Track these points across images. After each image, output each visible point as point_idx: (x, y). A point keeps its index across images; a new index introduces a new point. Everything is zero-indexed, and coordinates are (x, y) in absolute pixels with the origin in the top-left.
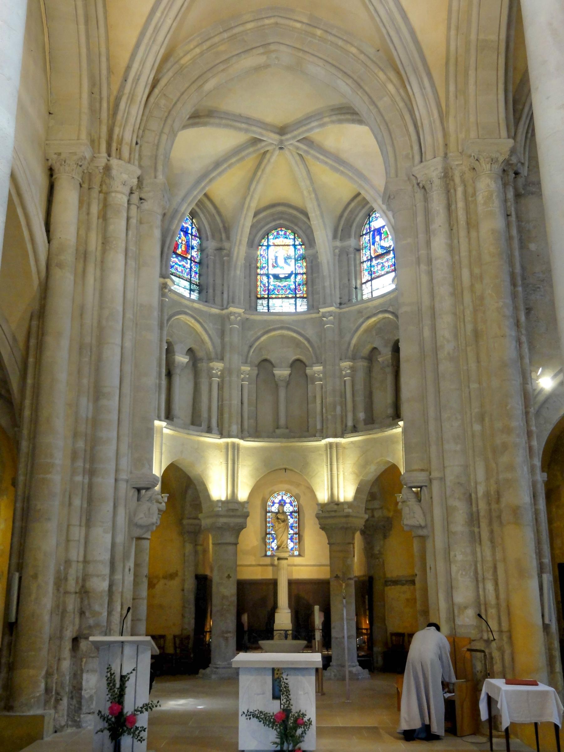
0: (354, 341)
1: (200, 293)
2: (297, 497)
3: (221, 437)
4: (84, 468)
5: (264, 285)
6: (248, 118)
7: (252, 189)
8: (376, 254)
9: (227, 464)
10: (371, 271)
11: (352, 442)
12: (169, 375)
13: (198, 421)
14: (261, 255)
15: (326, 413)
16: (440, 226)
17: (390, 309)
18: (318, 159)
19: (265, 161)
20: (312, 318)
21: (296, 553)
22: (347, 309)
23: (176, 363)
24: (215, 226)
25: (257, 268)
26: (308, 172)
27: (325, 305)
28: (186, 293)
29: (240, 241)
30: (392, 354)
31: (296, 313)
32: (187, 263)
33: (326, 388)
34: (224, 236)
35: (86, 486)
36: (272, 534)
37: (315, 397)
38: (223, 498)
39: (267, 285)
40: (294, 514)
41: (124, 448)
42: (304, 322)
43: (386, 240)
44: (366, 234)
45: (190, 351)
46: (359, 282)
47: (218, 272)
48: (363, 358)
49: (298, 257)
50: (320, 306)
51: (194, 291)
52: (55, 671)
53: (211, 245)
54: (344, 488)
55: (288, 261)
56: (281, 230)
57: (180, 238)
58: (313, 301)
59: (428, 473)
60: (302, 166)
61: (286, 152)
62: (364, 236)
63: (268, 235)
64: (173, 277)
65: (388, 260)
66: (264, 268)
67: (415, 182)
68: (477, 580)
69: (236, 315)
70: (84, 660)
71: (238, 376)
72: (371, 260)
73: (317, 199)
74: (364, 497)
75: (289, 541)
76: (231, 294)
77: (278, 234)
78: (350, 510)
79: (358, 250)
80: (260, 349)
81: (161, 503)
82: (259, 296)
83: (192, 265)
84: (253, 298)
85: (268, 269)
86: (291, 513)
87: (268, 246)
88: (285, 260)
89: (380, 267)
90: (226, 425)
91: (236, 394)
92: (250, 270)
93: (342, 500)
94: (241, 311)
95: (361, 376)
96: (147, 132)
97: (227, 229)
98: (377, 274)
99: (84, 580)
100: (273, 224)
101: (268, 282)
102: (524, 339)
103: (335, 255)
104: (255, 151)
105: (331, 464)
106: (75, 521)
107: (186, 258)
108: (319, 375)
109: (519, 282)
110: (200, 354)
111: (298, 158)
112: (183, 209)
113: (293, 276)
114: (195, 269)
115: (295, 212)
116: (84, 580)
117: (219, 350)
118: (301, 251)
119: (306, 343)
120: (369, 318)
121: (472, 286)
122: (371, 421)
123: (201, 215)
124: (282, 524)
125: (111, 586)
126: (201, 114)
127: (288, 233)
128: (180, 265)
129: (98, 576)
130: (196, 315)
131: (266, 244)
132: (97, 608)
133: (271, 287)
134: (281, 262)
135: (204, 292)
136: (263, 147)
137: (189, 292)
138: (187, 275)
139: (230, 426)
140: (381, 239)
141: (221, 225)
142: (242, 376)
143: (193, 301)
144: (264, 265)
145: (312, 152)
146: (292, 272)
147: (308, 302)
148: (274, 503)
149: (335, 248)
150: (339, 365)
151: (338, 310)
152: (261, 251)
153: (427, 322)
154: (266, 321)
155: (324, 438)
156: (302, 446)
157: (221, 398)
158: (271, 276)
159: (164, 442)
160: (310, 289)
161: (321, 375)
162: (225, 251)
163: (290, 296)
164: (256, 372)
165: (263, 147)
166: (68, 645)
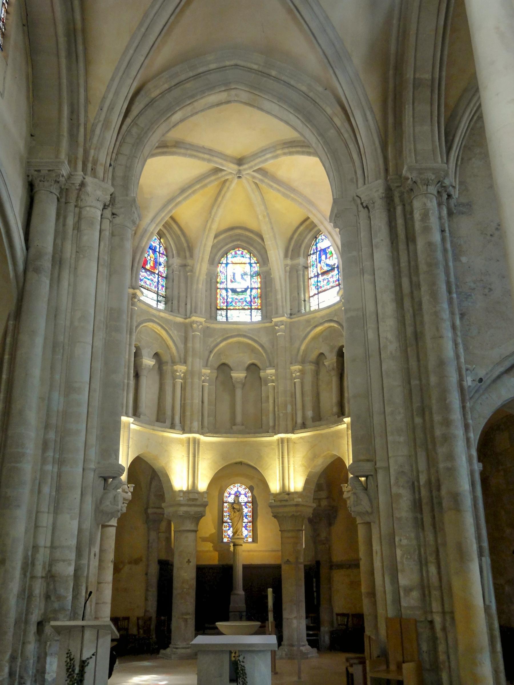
0: (303, 347)
1: (165, 304)
2: (251, 489)
3: (183, 433)
4: (54, 458)
5: (224, 299)
6: (210, 150)
7: (213, 214)
8: (322, 271)
9: (189, 457)
10: (318, 286)
11: (301, 438)
12: (137, 376)
13: (162, 418)
14: (221, 272)
15: (278, 411)
16: (382, 240)
17: (335, 319)
18: (271, 187)
19: (225, 189)
20: (266, 327)
21: (250, 540)
22: (296, 319)
23: (144, 365)
24: (181, 246)
25: (217, 283)
26: (263, 199)
27: (277, 315)
28: (154, 304)
29: (202, 258)
30: (337, 358)
31: (252, 323)
32: (155, 278)
33: (278, 388)
34: (188, 254)
35: (56, 475)
36: (228, 522)
37: (268, 397)
38: (185, 489)
39: (226, 298)
40: (248, 504)
41: (93, 440)
42: (258, 330)
43: (331, 258)
44: (313, 254)
45: (157, 355)
46: (307, 296)
47: (182, 285)
48: (311, 362)
49: (253, 274)
50: (272, 316)
51: (160, 302)
52: (19, 655)
53: (176, 262)
54: (294, 479)
55: (245, 277)
56: (239, 250)
57: (149, 255)
58: (266, 312)
59: (373, 463)
60: (257, 193)
61: (243, 180)
62: (312, 256)
63: (227, 254)
64: (142, 289)
65: (332, 277)
66: (223, 283)
67: (359, 202)
68: (422, 563)
69: (198, 324)
70: (48, 643)
71: (199, 379)
72: (318, 276)
73: (271, 223)
74: (313, 487)
75: (244, 529)
76: (193, 305)
77: (236, 253)
78: (300, 500)
79: (306, 268)
80: (219, 354)
81: (127, 493)
82: (218, 308)
83: (159, 279)
84: (213, 309)
85: (226, 284)
86: (246, 503)
87: (227, 264)
88: (242, 276)
89: (326, 282)
90: (188, 422)
91: (197, 394)
92: (211, 285)
93: (292, 490)
94: (203, 320)
95: (309, 378)
96: (119, 156)
97: (191, 249)
98: (323, 289)
99: (50, 565)
100: (232, 244)
101: (227, 295)
102: (459, 340)
103: (286, 272)
104: (216, 179)
105: (283, 458)
106: (44, 508)
107: (154, 273)
108: (271, 377)
109: (454, 290)
110: (166, 358)
111: (254, 186)
112: (152, 228)
113: (249, 290)
114: (163, 282)
115: (251, 235)
116: (50, 565)
117: (182, 356)
118: (256, 268)
119: (260, 349)
120: (316, 327)
121: (412, 292)
122: (318, 419)
123: (168, 236)
124: (238, 513)
125: (76, 570)
126: (168, 144)
127: (244, 253)
128: (148, 279)
129: (64, 561)
130: (164, 324)
131: (225, 262)
132: (62, 592)
133: (229, 300)
134: (238, 277)
135: (170, 303)
136: (222, 176)
137: (156, 302)
138: (155, 287)
139: (191, 423)
140: (326, 258)
141: (185, 245)
142: (203, 378)
143: (160, 311)
144: (223, 281)
145: (266, 180)
146: (248, 286)
147: (262, 314)
148: (230, 494)
149: (286, 265)
150: (290, 369)
151: (289, 320)
152: (221, 268)
153: (371, 325)
154: (224, 329)
155: (276, 434)
156: (256, 441)
157: (183, 398)
158: (229, 290)
159: (131, 436)
160: (264, 301)
161: (274, 378)
162: (189, 267)
163: (246, 307)
164: (215, 375)
165: (222, 176)
166: (33, 628)
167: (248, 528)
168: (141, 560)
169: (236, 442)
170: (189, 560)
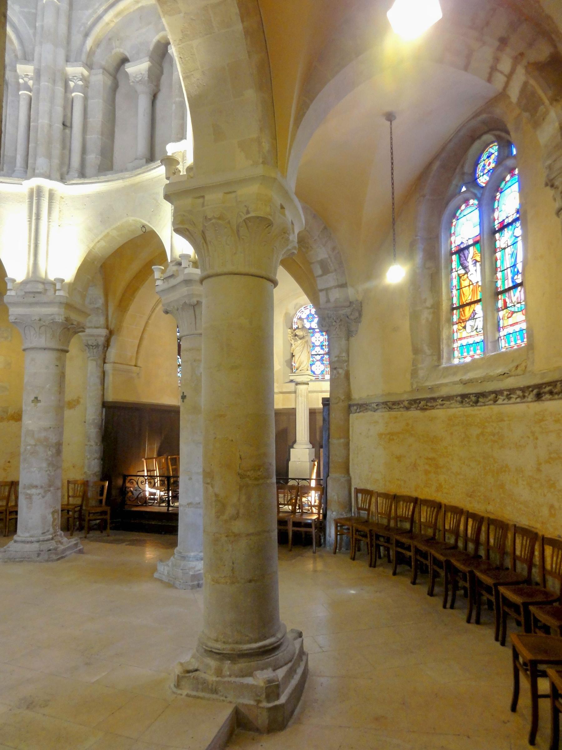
80: (109, 39)
124: (300, 341)
167: (325, 362)
170: (36, 398)
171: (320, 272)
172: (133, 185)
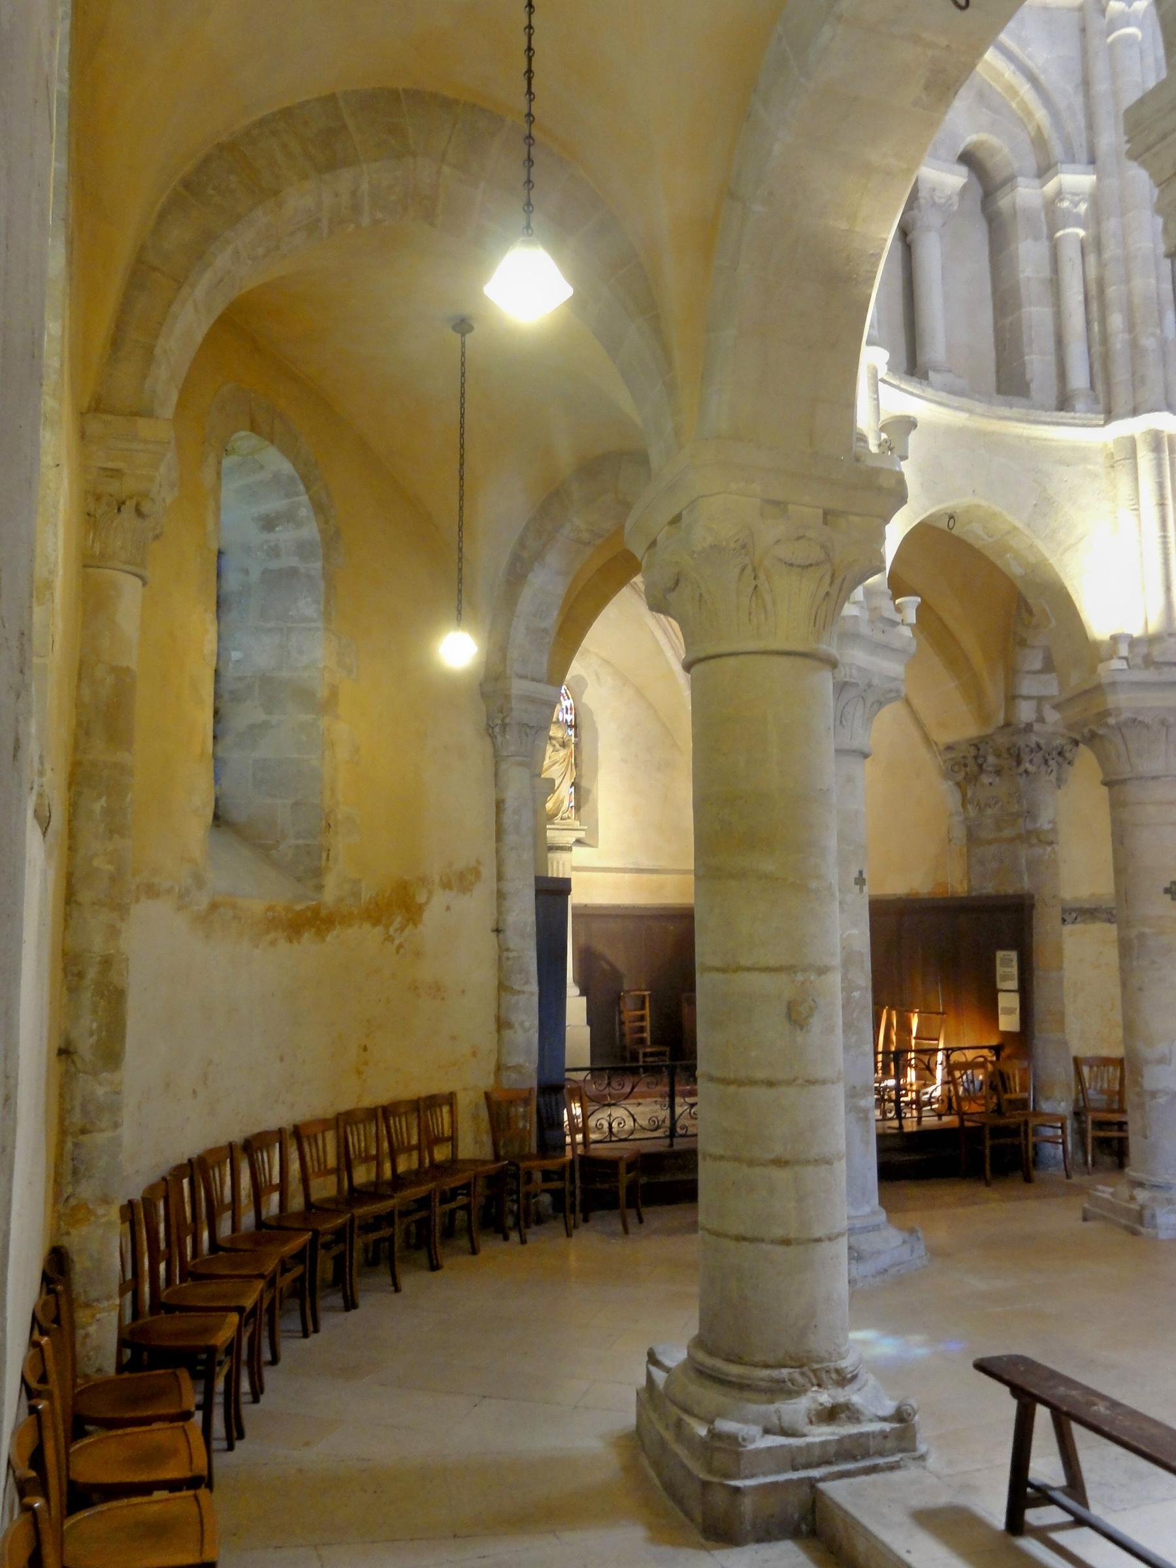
108: (1076, 205)
119: (1025, 90)
161: (1083, 207)
168: (478, 874)
169: (962, 431)
171: (1038, 665)
172: (980, 433)
